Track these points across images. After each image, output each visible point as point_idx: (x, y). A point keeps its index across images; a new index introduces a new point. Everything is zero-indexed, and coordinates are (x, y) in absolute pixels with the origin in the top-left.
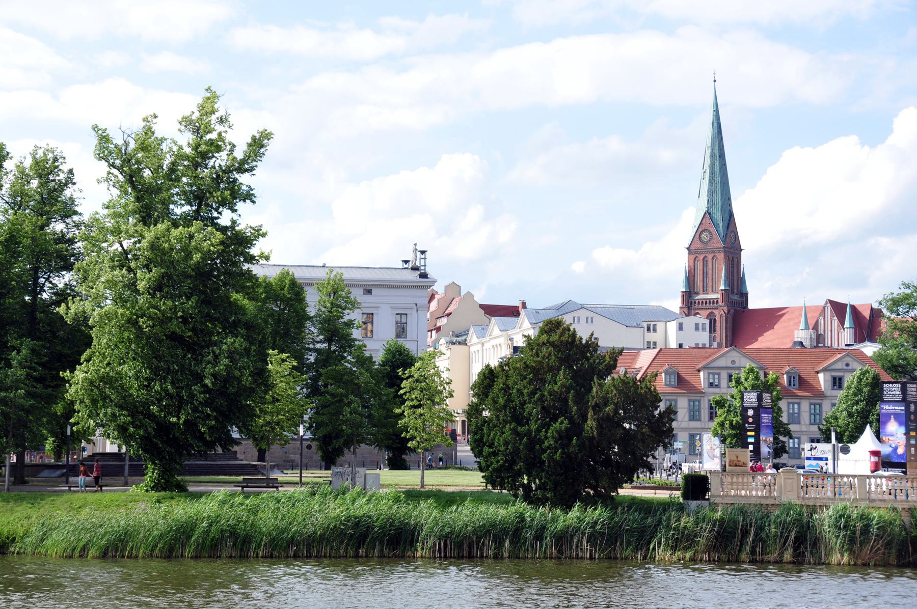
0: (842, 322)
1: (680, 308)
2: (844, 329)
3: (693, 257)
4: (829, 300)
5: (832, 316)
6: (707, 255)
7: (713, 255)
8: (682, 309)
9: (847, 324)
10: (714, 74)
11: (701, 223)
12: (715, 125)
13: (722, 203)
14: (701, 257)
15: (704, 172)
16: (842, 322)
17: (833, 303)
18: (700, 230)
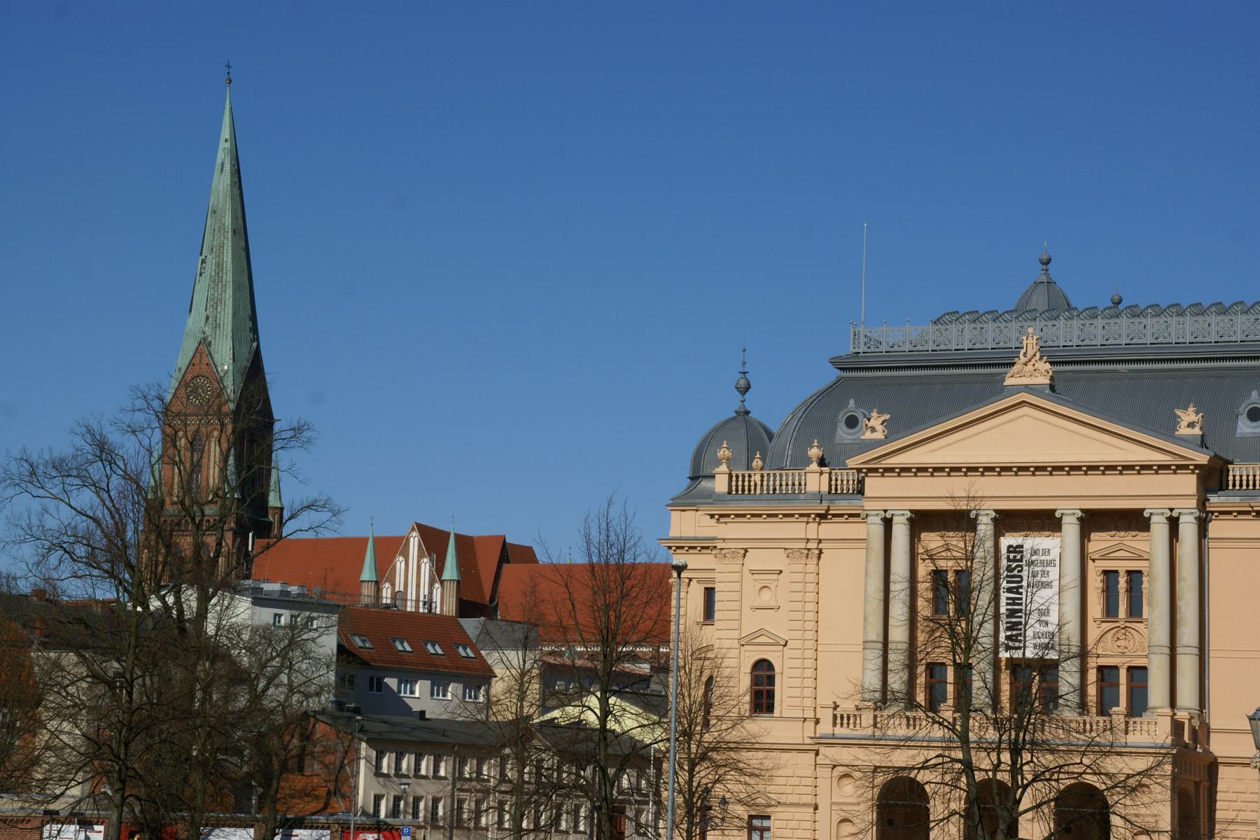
0: (439, 569)
2: (442, 582)
4: (417, 524)
5: (420, 557)
9: (450, 572)
10: (228, 66)
11: (191, 364)
12: (227, 167)
13: (234, 323)
15: (203, 262)
16: (439, 569)
17: (426, 533)
18: (189, 377)
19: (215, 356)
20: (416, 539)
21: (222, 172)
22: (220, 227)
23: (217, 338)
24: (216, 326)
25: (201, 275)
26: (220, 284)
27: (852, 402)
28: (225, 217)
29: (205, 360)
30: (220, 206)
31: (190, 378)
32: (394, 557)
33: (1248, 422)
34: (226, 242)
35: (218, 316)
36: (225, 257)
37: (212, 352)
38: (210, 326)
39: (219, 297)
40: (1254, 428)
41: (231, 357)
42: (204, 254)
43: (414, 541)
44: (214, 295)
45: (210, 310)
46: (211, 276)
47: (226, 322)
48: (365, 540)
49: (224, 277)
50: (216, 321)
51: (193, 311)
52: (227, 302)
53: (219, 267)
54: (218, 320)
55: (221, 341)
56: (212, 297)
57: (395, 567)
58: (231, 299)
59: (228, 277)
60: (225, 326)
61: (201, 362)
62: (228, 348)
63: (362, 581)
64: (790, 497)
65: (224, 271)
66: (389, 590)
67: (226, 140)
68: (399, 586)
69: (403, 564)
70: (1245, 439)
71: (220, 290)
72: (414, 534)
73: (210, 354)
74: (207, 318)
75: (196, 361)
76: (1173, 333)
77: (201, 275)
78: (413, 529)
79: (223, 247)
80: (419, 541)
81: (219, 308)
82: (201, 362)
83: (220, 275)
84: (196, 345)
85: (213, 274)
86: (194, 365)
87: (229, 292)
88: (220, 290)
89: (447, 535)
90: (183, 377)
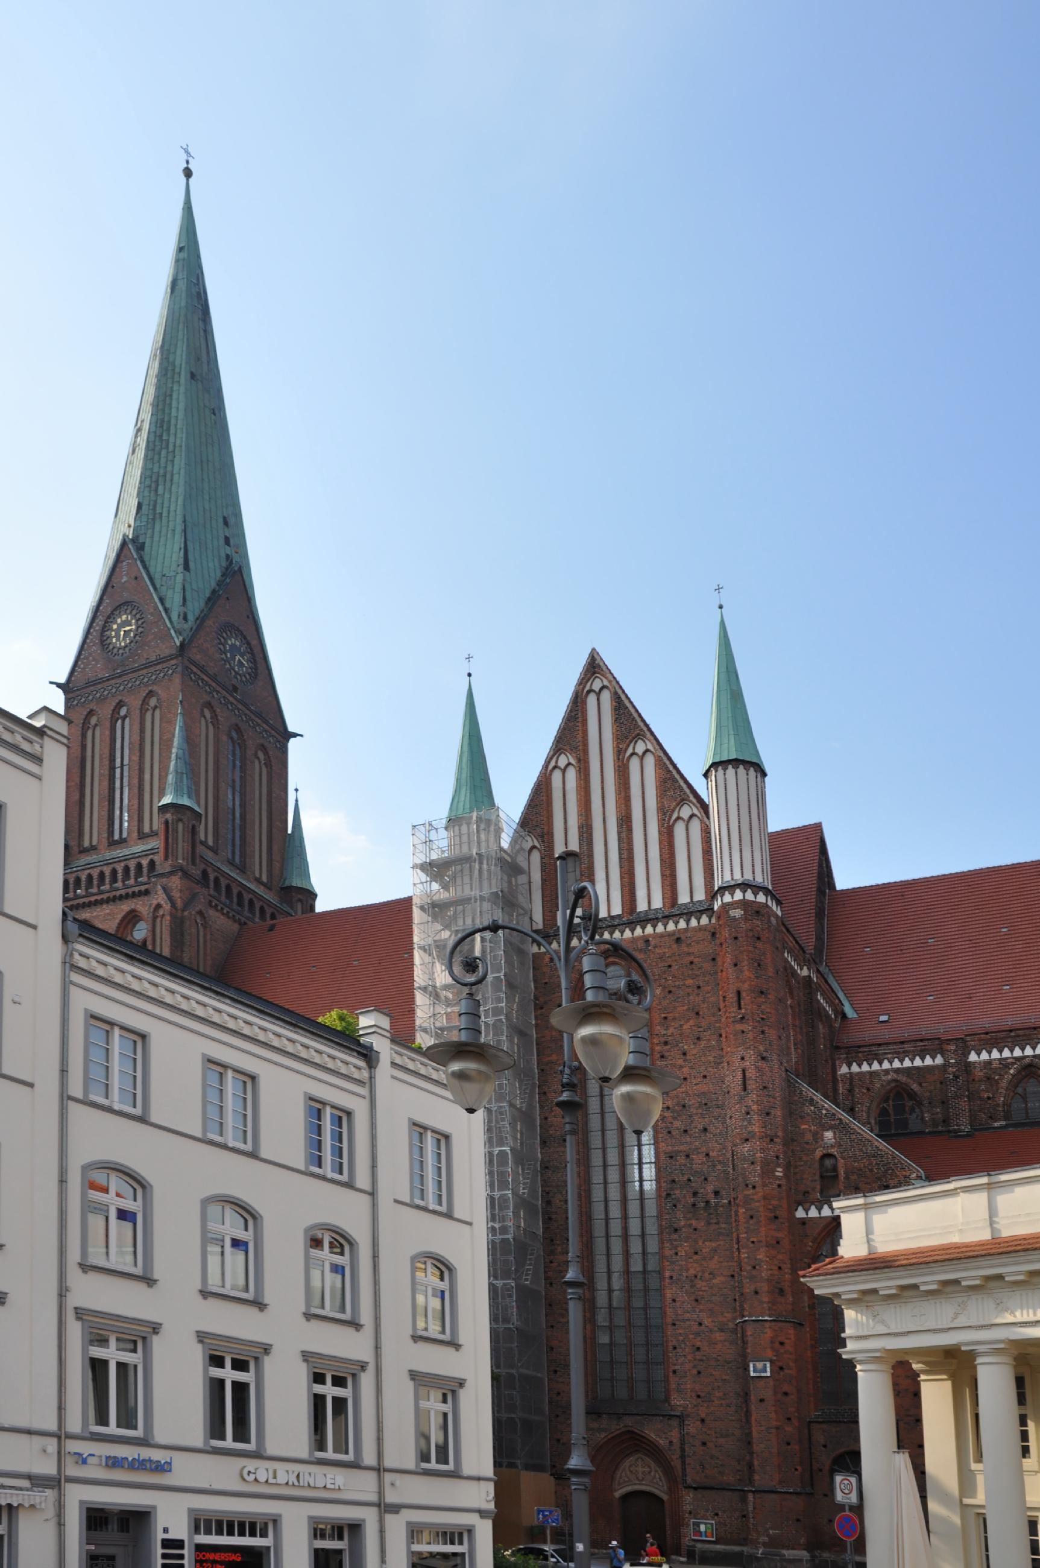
26: (164, 452)
28: (175, 353)
34: (175, 388)
35: (159, 501)
37: (146, 559)
38: (144, 519)
39: (162, 471)
41: (182, 561)
44: (152, 469)
46: (148, 441)
47: (172, 508)
49: (172, 440)
52: (176, 477)
53: (162, 426)
55: (163, 539)
58: (182, 471)
59: (179, 437)
60: (172, 514)
62: (176, 548)
65: (172, 431)
71: (163, 460)
74: (139, 507)
79: (171, 396)
81: (160, 488)
83: (165, 437)
85: (152, 436)
87: (180, 461)
88: (163, 460)
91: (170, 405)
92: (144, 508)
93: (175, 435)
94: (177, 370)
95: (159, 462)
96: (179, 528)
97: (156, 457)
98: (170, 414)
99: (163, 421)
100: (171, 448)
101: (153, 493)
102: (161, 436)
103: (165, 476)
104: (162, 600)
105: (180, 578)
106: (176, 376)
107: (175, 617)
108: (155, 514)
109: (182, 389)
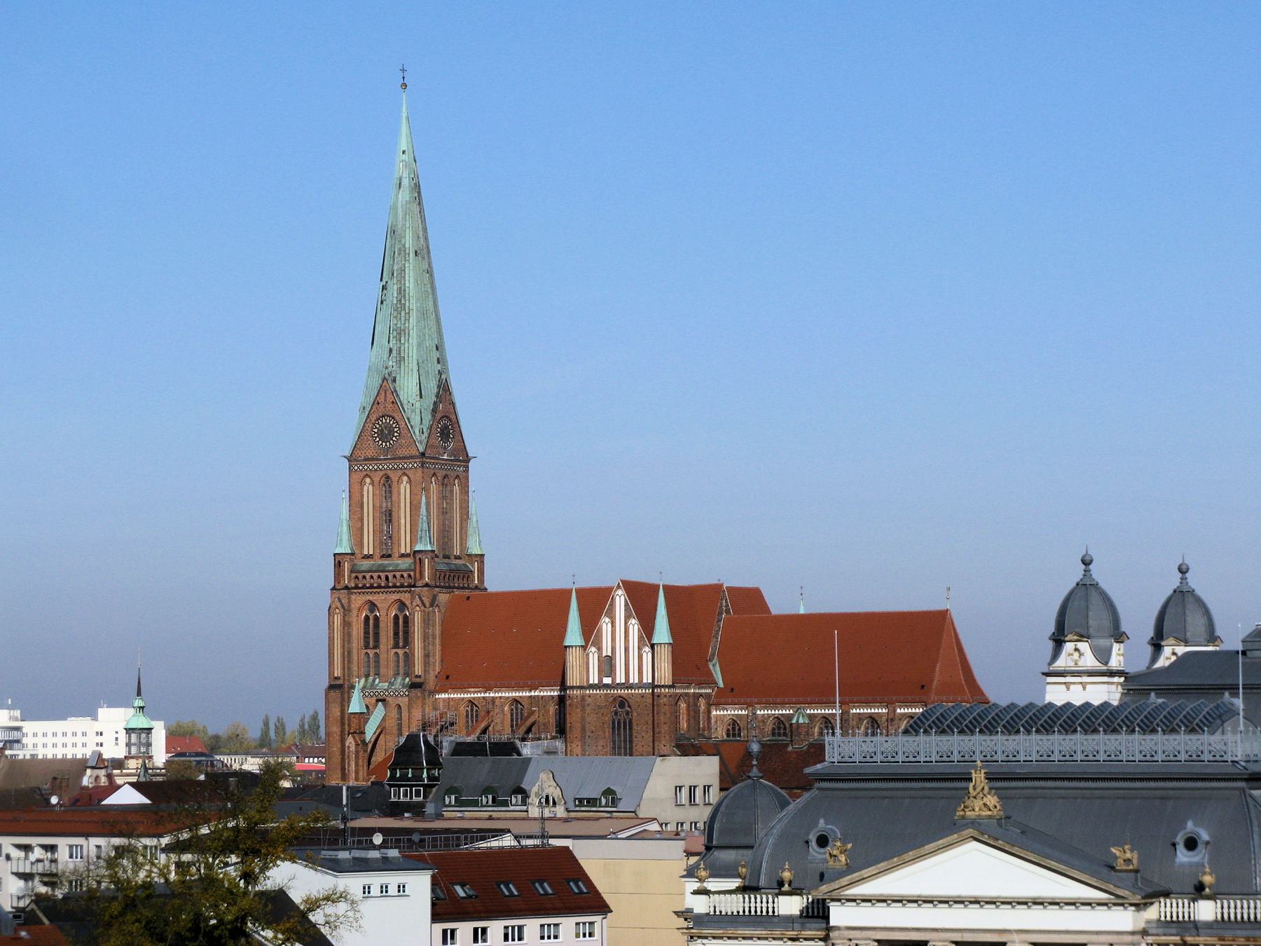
0: (648, 628)
1: (334, 589)
3: (357, 477)
5: (627, 618)
6: (389, 473)
7: (400, 473)
8: (337, 594)
9: (662, 633)
10: (403, 70)
11: (376, 402)
14: (377, 477)
16: (648, 628)
17: (632, 588)
19: (401, 394)
20: (623, 597)
21: (400, 187)
22: (400, 249)
23: (402, 371)
24: (400, 360)
25: (382, 303)
26: (403, 313)
27: (822, 821)
29: (390, 398)
30: (399, 226)
31: (375, 418)
32: (599, 618)
33: (1185, 851)
34: (406, 266)
35: (402, 348)
36: (407, 282)
40: (1190, 857)
42: (384, 280)
43: (620, 600)
45: (393, 342)
48: (570, 591)
49: (407, 304)
50: (400, 354)
51: (374, 345)
52: (411, 331)
54: (402, 351)
56: (395, 327)
57: (600, 631)
60: (410, 359)
61: (385, 400)
63: (566, 647)
64: (763, 919)
65: (407, 298)
66: (596, 655)
67: (404, 152)
68: (607, 651)
69: (610, 625)
70: (1182, 865)
71: (403, 319)
72: (620, 592)
73: (396, 391)
74: (391, 350)
75: (381, 399)
76: (1124, 751)
77: (382, 303)
78: (619, 587)
79: (405, 270)
80: (625, 599)
81: (402, 339)
82: (385, 400)
83: (403, 302)
84: (380, 382)
86: (378, 403)
88: (403, 319)
89: (658, 586)
90: (368, 417)
91: (404, 277)
92: (394, 352)
93: (409, 300)
94: (407, 251)
95: (400, 319)
96: (415, 368)
97: (399, 315)
98: (405, 284)
99: (400, 288)
100: (407, 311)
101: (398, 342)
102: (400, 301)
103: (404, 330)
104: (408, 419)
105: (418, 405)
106: (407, 256)
107: (417, 432)
108: (400, 356)
109: (411, 267)
